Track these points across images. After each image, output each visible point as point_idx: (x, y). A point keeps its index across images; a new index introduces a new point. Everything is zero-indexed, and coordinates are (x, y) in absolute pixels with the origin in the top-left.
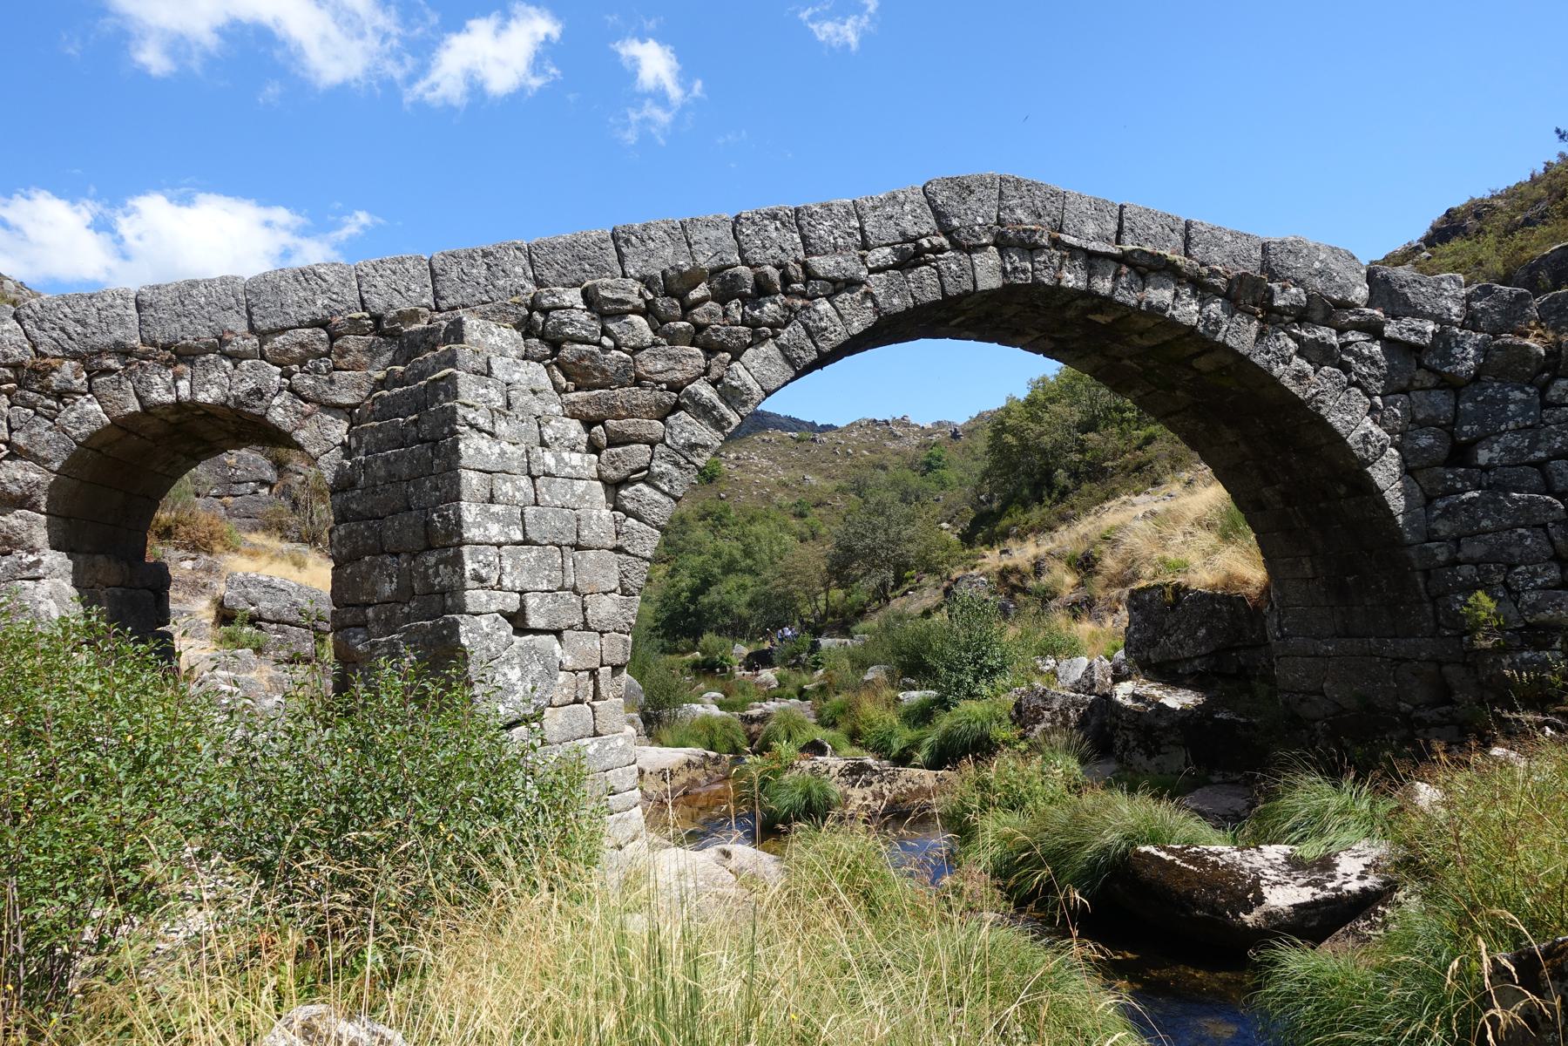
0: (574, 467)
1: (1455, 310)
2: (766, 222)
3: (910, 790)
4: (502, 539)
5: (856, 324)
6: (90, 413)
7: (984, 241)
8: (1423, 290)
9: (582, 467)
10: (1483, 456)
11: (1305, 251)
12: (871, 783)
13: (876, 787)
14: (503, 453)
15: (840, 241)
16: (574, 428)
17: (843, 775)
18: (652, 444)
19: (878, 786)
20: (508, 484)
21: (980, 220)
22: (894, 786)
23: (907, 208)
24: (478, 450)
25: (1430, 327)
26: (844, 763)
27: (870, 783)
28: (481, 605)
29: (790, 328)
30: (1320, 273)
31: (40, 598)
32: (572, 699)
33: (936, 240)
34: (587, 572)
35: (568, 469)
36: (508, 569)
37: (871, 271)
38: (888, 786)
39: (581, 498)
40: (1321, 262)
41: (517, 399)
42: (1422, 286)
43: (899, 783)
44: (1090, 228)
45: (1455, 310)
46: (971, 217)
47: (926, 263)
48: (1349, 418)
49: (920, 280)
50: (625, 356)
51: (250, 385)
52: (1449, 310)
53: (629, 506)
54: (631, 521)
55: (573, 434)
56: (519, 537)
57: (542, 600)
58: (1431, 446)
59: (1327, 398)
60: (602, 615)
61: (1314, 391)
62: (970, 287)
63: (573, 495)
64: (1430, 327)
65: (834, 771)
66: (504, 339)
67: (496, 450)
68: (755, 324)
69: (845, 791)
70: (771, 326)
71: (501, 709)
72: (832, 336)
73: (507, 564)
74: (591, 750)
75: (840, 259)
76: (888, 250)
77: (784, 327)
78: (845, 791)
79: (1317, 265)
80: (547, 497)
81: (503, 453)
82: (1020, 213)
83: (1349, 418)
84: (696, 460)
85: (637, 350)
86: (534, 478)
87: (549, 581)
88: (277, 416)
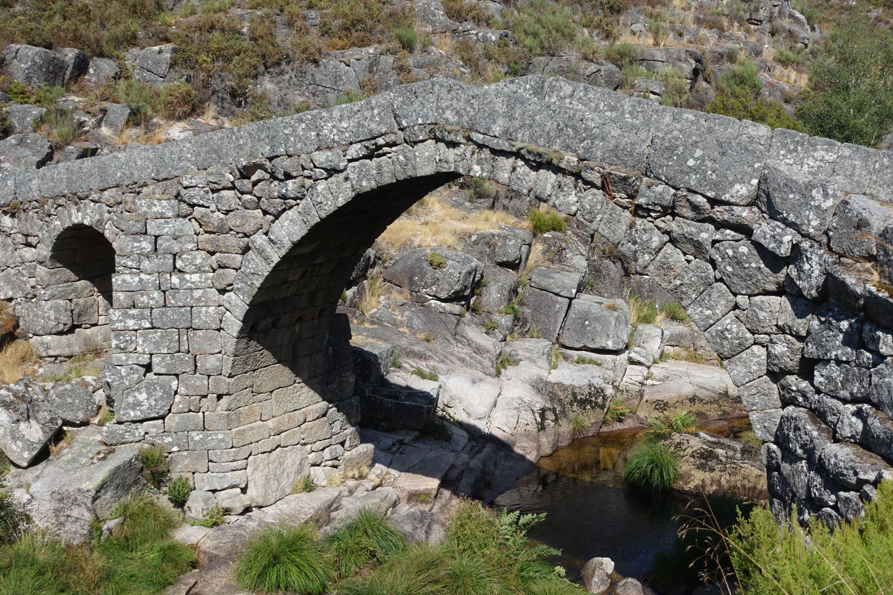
0: (192, 283)
1: (814, 223)
2: (297, 125)
3: (744, 486)
4: (136, 328)
5: (340, 199)
6: (58, 225)
7: (421, 138)
8: (791, 196)
9: (201, 282)
10: (818, 379)
11: (681, 148)
12: (714, 470)
13: (716, 474)
14: (141, 280)
15: (336, 138)
16: (200, 257)
17: (693, 457)
18: (237, 270)
19: (719, 474)
20: (145, 297)
21: (420, 121)
22: (733, 478)
23: (376, 112)
24: (124, 281)
25: (789, 237)
26: (700, 445)
27: (712, 470)
28: (122, 361)
29: (304, 201)
30: (693, 170)
31: (46, 310)
32: (186, 410)
33: (391, 138)
34: (197, 343)
35: (189, 284)
36: (141, 343)
37: (350, 161)
38: (728, 477)
39: (199, 300)
40: (696, 159)
41: (161, 245)
42: (793, 192)
43: (739, 477)
44: (497, 129)
45: (814, 223)
46: (414, 118)
47: (384, 154)
48: (708, 312)
49: (379, 168)
50: (222, 216)
51: (97, 217)
52: (809, 221)
53: (227, 305)
54: (228, 313)
55: (198, 261)
56: (148, 325)
57: (163, 359)
58: (783, 354)
59: (690, 291)
60: (208, 366)
61: (678, 282)
62: (410, 173)
63: (192, 298)
64: (789, 237)
65: (690, 451)
66: (163, 208)
67: (137, 279)
68: (284, 197)
69: (690, 470)
70: (295, 199)
71: (132, 413)
72: (326, 208)
73: (140, 342)
74: (197, 438)
75: (329, 153)
76: (359, 146)
77: (301, 199)
78: (690, 470)
79: (691, 162)
80: (173, 302)
81: (141, 280)
82: (449, 115)
83: (708, 312)
84: (255, 282)
85: (227, 212)
86: (164, 292)
87: (169, 349)
88: (107, 234)
